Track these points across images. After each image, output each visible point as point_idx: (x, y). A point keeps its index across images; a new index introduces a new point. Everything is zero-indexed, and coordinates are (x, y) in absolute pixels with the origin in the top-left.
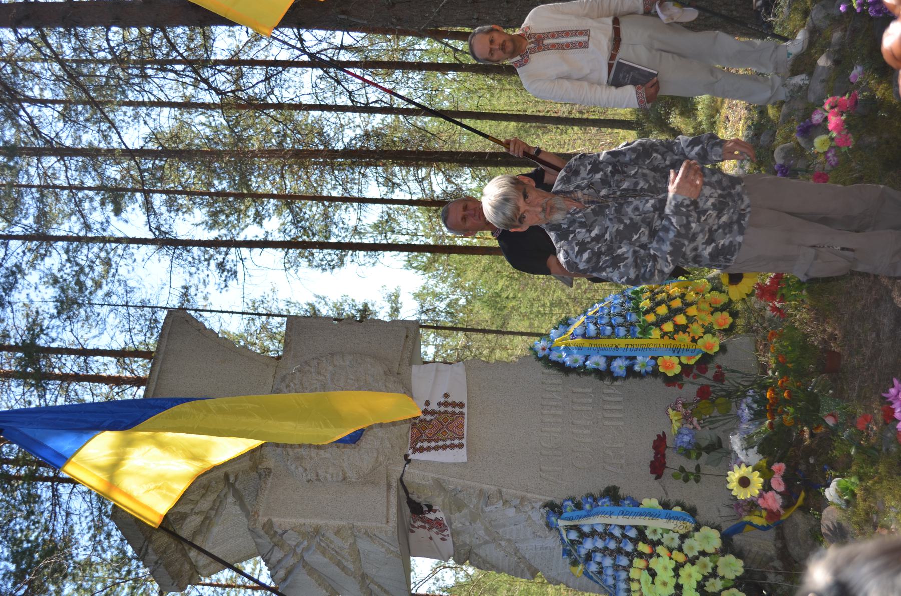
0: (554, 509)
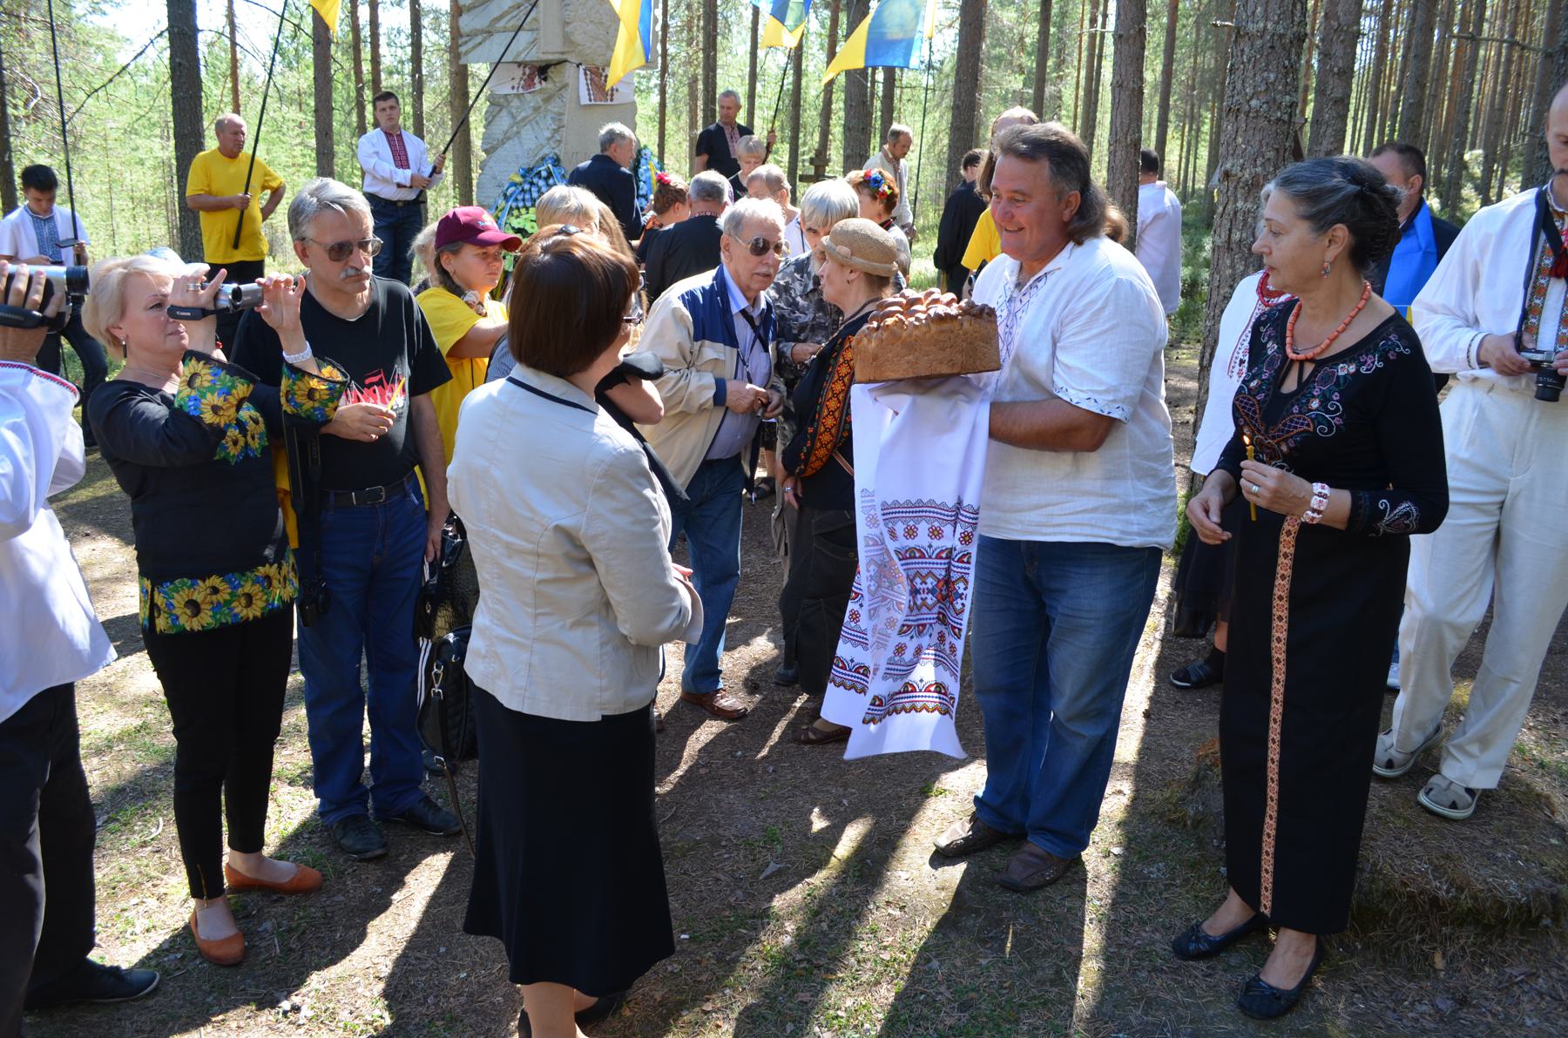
0: (557, 162)
